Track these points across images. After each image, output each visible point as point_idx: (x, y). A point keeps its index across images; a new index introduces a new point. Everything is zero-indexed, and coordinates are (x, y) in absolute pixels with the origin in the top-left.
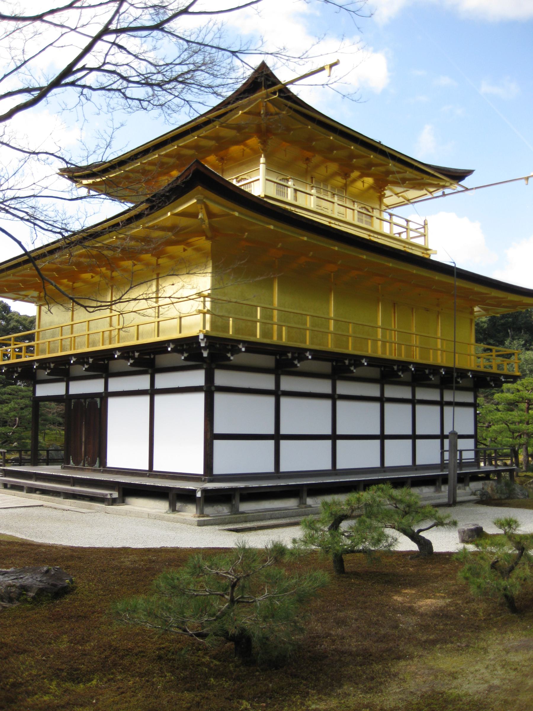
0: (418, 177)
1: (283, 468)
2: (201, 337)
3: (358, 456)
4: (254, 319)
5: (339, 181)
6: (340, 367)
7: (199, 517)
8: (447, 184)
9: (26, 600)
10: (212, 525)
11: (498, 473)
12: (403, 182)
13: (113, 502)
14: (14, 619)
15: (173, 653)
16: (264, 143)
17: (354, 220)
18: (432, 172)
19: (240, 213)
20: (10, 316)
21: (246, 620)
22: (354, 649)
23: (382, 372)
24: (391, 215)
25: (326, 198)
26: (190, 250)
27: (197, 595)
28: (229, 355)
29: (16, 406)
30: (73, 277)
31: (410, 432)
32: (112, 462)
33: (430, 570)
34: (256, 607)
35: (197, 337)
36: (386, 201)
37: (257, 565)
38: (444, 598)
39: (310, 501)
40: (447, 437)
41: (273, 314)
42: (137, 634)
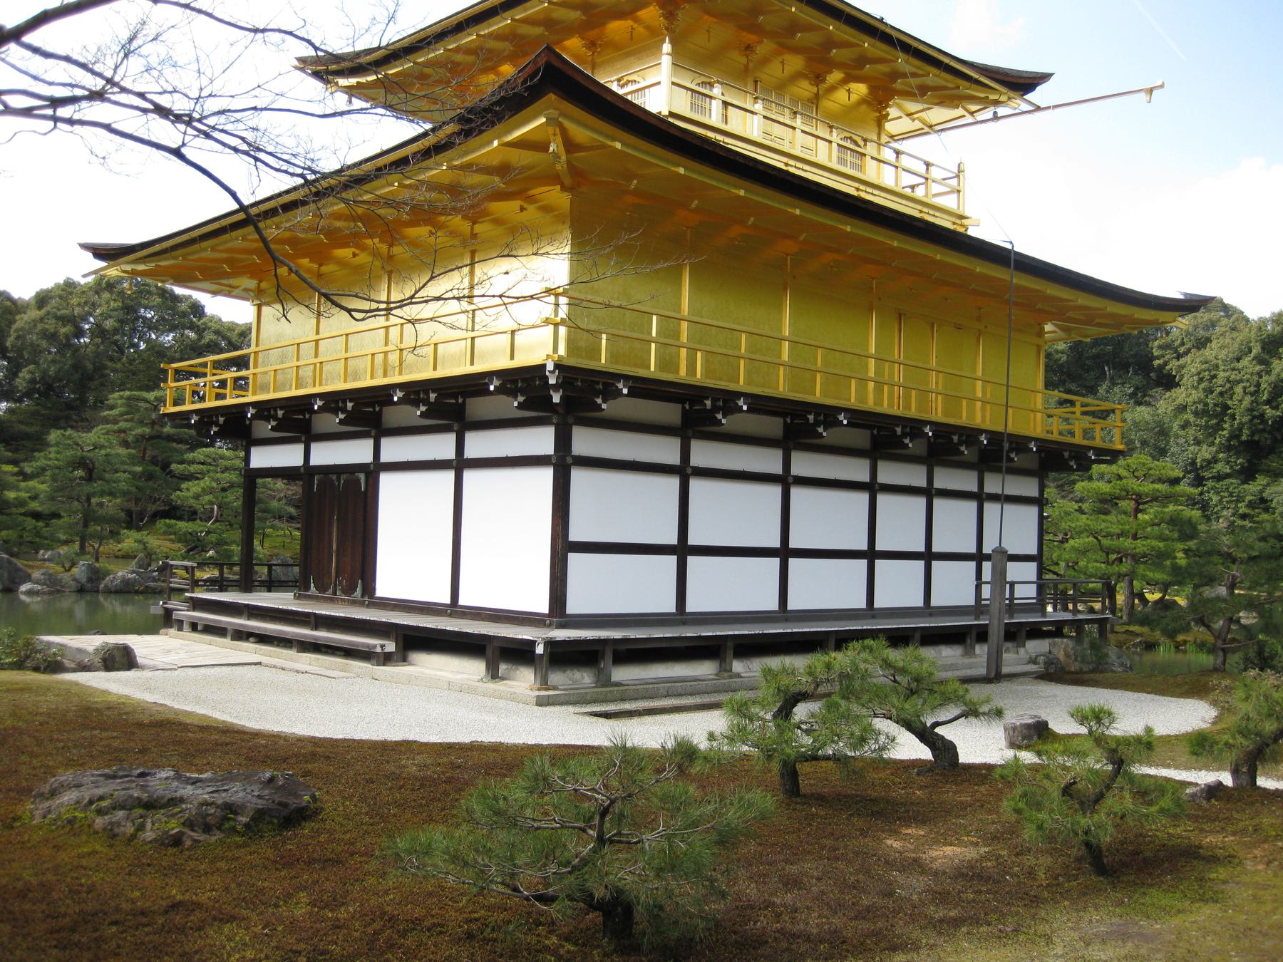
0: (950, 85)
1: (691, 607)
2: (550, 367)
3: (825, 589)
4: (648, 338)
5: (805, 88)
6: (798, 426)
7: (539, 690)
8: (1003, 98)
9: (233, 829)
10: (561, 704)
11: (1078, 625)
12: (920, 93)
13: (386, 659)
14: (212, 862)
15: (493, 929)
16: (670, 16)
17: (830, 159)
18: (975, 76)
19: (623, 144)
20: (205, 324)
21: (625, 874)
22: (815, 931)
23: (874, 438)
24: (898, 153)
25: (781, 120)
26: (531, 209)
27: (538, 828)
28: (599, 401)
29: (214, 484)
30: (320, 254)
31: (921, 548)
32: (385, 587)
33: (951, 793)
34: (643, 851)
35: (544, 366)
36: (890, 127)
37: (647, 777)
38: (976, 844)
39: (738, 666)
40: (988, 557)
41: (682, 327)
42: (430, 894)
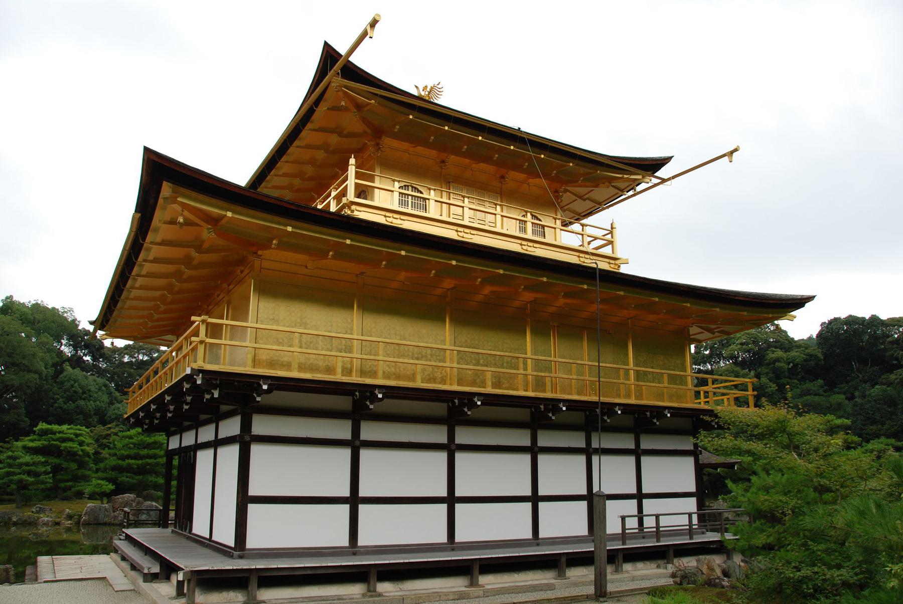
3: (479, 526)
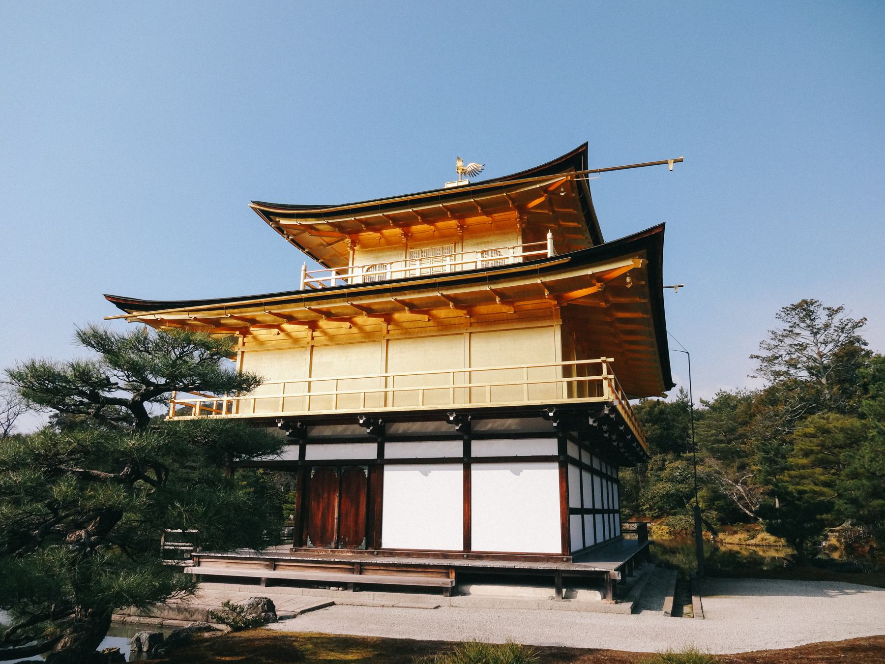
13: (454, 592)
32: (388, 541)
